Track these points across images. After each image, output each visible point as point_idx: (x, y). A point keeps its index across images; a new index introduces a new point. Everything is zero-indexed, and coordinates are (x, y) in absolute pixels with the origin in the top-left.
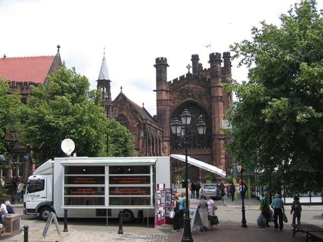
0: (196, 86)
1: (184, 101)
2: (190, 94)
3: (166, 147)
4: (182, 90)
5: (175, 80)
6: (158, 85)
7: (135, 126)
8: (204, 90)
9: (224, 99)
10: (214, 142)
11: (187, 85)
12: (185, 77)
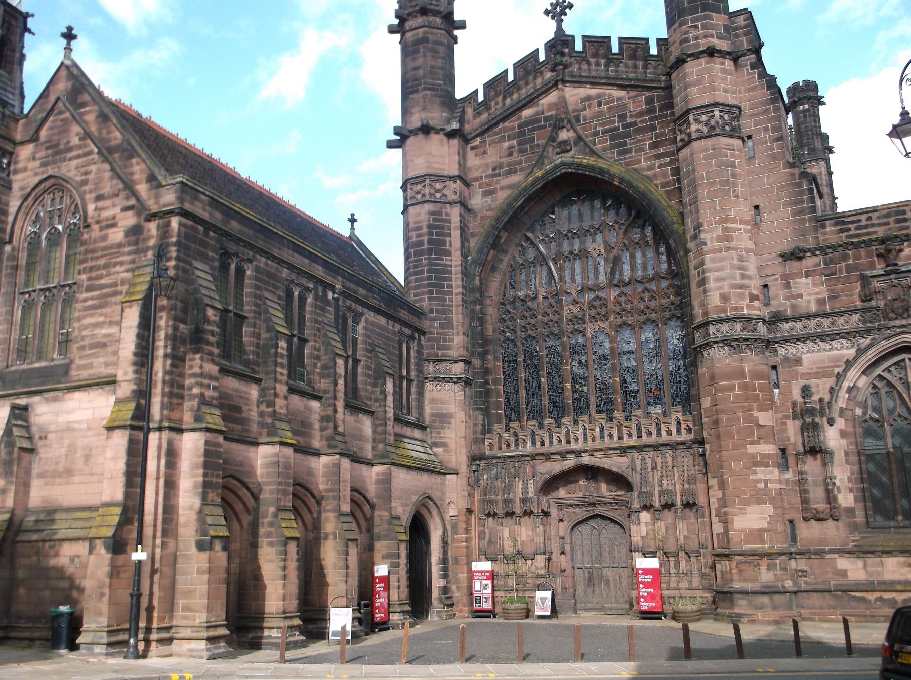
0: (593, 91)
1: (539, 173)
2: (564, 135)
3: (443, 419)
4: (528, 123)
5: (495, 85)
6: (406, 112)
7: (117, 235)
8: (635, 103)
9: (747, 125)
10: (702, 370)
11: (552, 97)
12: (542, 57)
